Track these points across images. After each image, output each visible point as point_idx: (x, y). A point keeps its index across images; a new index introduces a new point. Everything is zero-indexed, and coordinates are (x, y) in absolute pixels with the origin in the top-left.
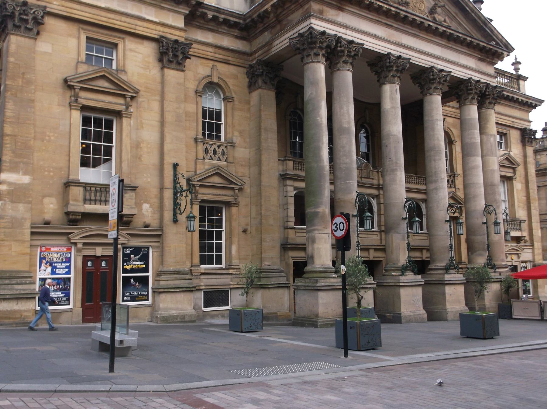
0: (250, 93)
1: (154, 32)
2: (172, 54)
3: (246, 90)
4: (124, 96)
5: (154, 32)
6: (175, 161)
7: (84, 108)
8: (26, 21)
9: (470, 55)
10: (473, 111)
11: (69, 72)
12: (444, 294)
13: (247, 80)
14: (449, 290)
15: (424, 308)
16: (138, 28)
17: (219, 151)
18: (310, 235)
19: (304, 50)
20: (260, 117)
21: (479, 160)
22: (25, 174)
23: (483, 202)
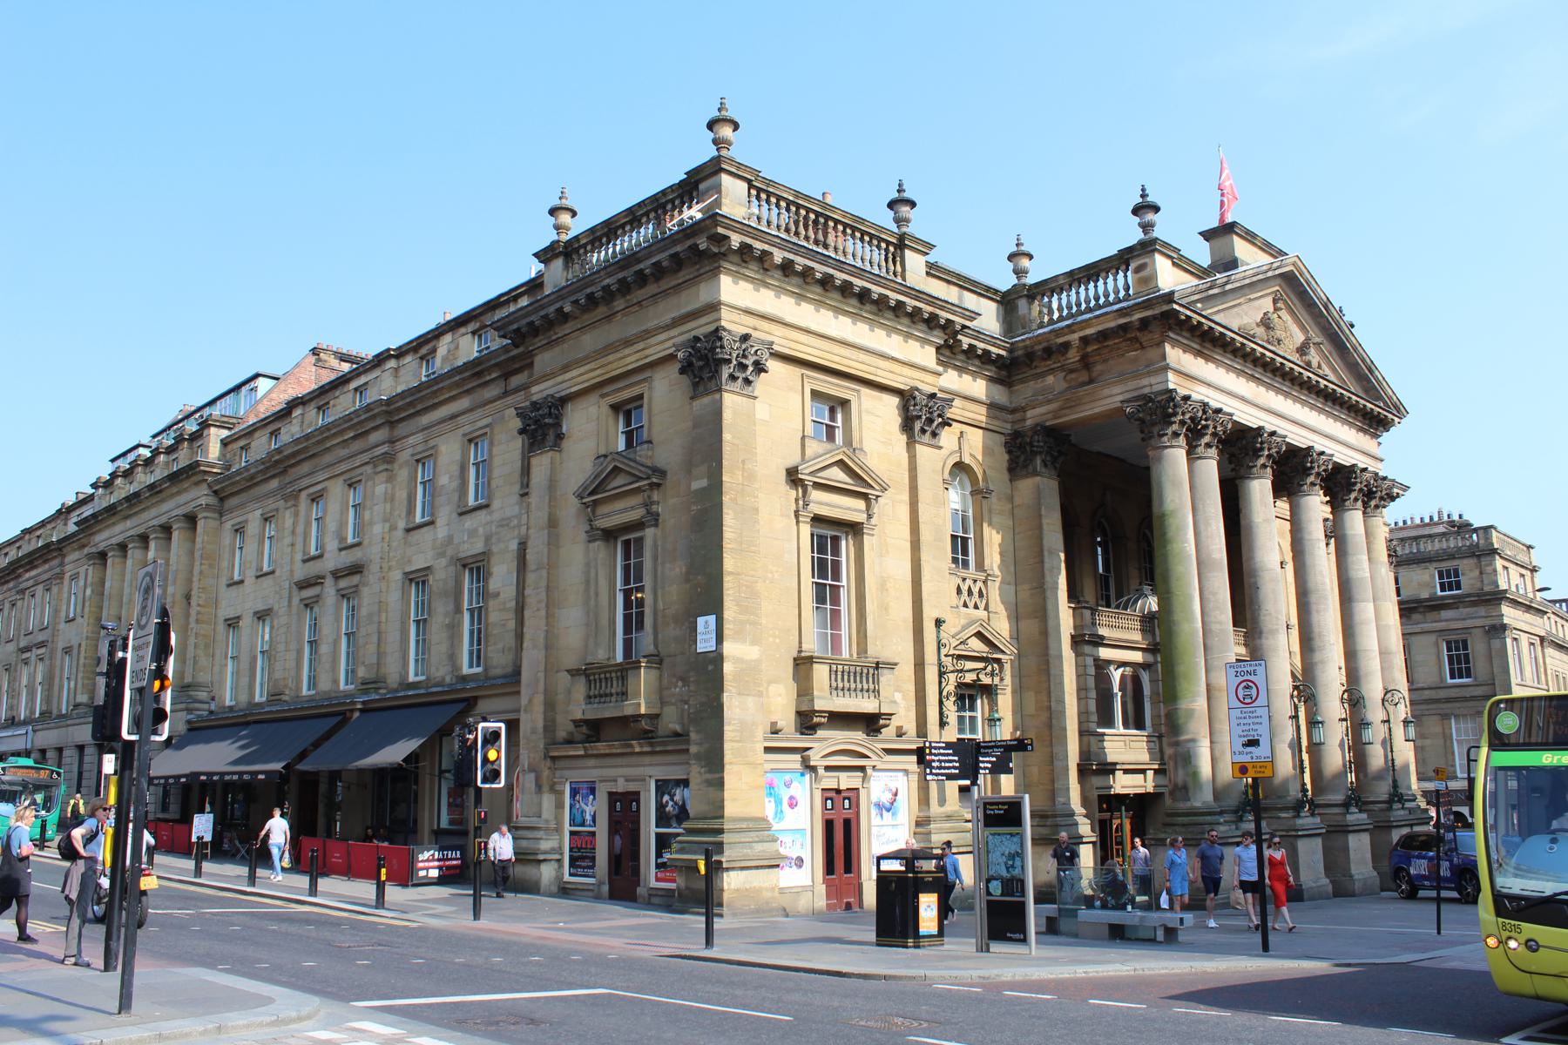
0: (692, 398)
1: (900, 379)
2: (921, 416)
3: (1006, 476)
4: (865, 496)
5: (900, 379)
6: (936, 615)
7: (817, 520)
8: (744, 367)
9: (1351, 425)
10: (1316, 505)
11: (793, 459)
12: (1346, 849)
13: (1006, 457)
14: (1353, 840)
15: (1327, 876)
16: (880, 372)
17: (975, 590)
18: (1180, 749)
19: (1154, 424)
20: (1040, 527)
21: (1370, 606)
22: (753, 643)
23: (1380, 686)
